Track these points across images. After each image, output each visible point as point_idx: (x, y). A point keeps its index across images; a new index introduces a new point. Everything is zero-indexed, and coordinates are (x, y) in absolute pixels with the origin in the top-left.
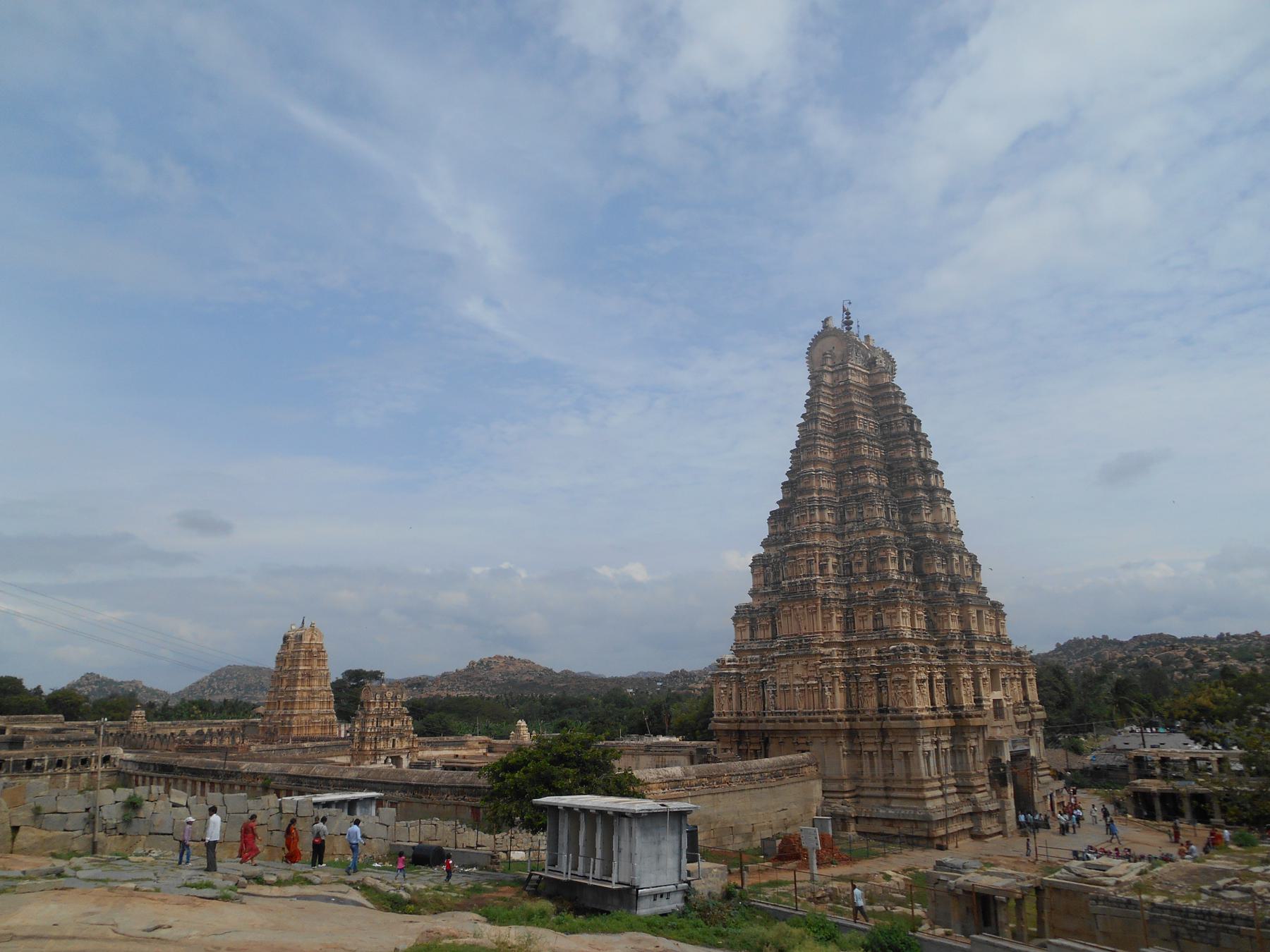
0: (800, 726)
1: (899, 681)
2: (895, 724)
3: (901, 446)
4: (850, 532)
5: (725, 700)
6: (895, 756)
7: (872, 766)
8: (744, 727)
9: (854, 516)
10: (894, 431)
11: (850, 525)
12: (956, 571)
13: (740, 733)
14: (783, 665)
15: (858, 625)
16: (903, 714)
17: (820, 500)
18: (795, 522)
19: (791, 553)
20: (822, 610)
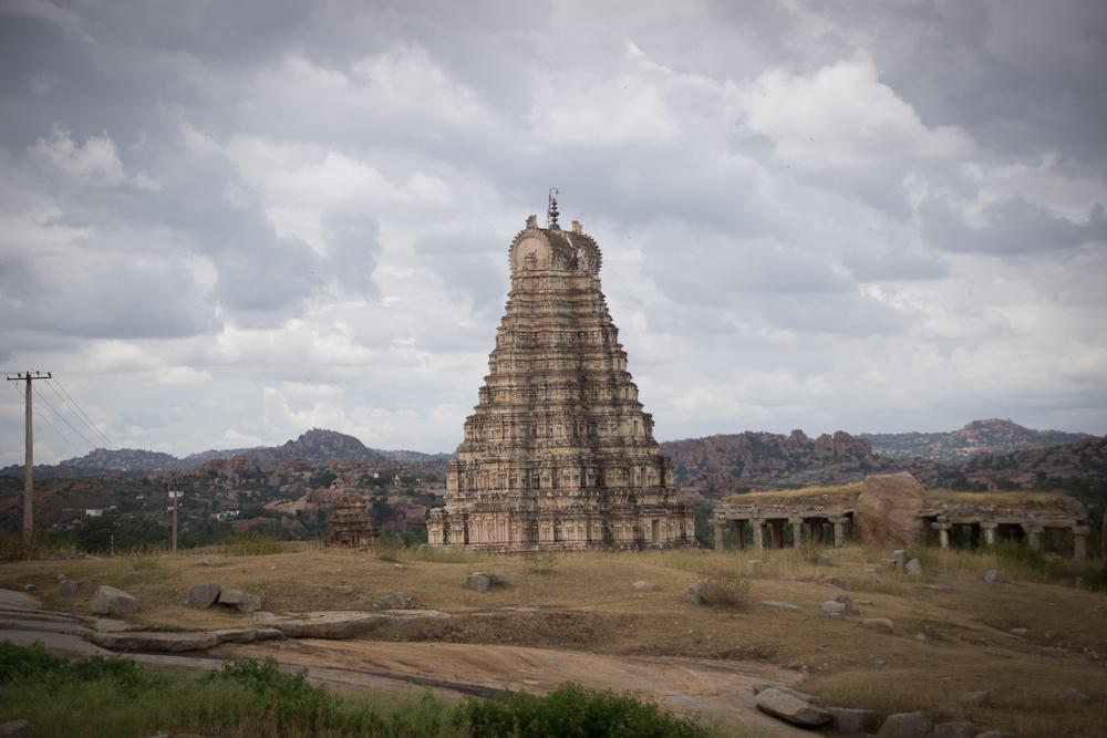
3: (596, 359)
10: (590, 341)
11: (540, 440)
12: (636, 483)
15: (542, 536)
17: (513, 416)
18: (490, 435)
20: (510, 522)
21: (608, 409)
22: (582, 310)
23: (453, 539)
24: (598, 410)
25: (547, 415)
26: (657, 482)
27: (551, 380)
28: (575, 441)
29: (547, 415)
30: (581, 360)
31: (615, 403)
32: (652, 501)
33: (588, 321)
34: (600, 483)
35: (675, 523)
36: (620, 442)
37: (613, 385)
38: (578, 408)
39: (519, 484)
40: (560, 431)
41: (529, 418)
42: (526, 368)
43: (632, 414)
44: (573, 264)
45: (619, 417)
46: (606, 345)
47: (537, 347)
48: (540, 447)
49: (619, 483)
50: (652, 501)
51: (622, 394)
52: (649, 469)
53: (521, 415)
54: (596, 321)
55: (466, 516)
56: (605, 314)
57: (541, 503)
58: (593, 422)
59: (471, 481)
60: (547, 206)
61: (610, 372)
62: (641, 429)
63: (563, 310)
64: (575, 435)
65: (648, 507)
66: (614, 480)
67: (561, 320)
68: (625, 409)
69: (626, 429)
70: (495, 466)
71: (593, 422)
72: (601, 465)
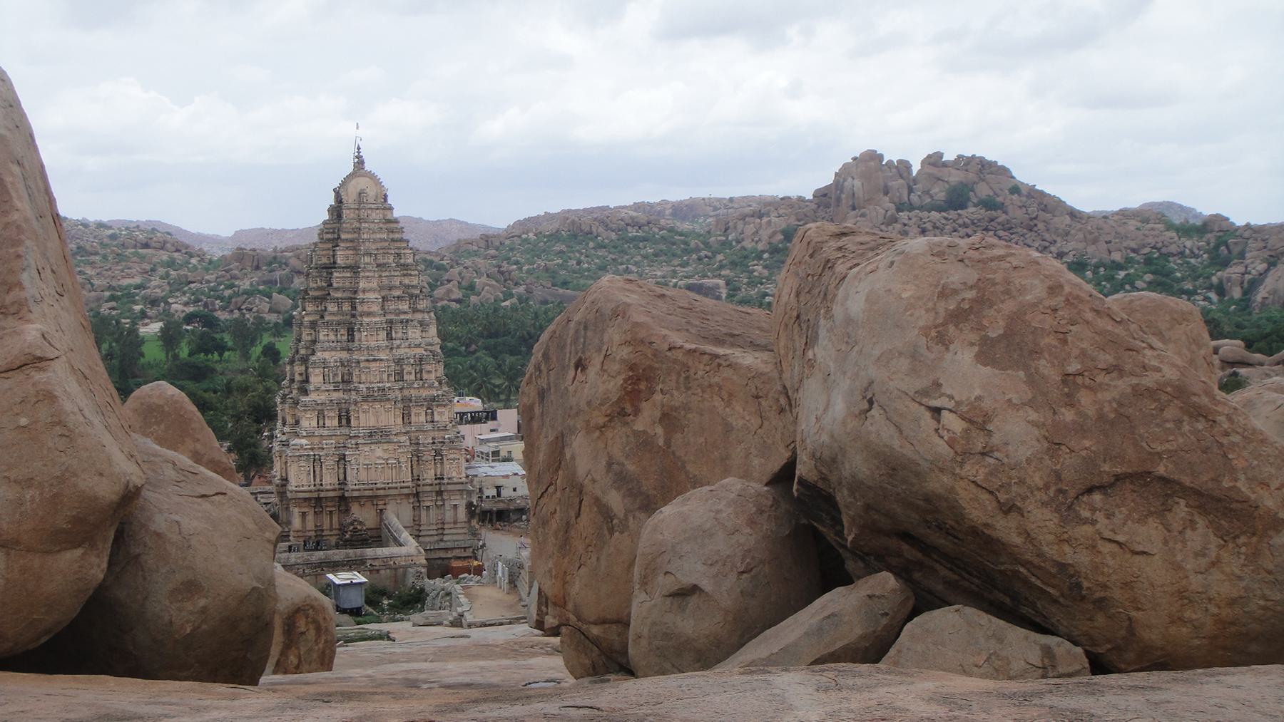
0: (382, 493)
1: (454, 459)
2: (450, 487)
4: (398, 347)
5: (304, 477)
6: (447, 506)
7: (428, 516)
8: (322, 494)
9: (400, 335)
11: (398, 342)
14: (367, 448)
15: (413, 419)
16: (455, 480)
19: (367, 364)
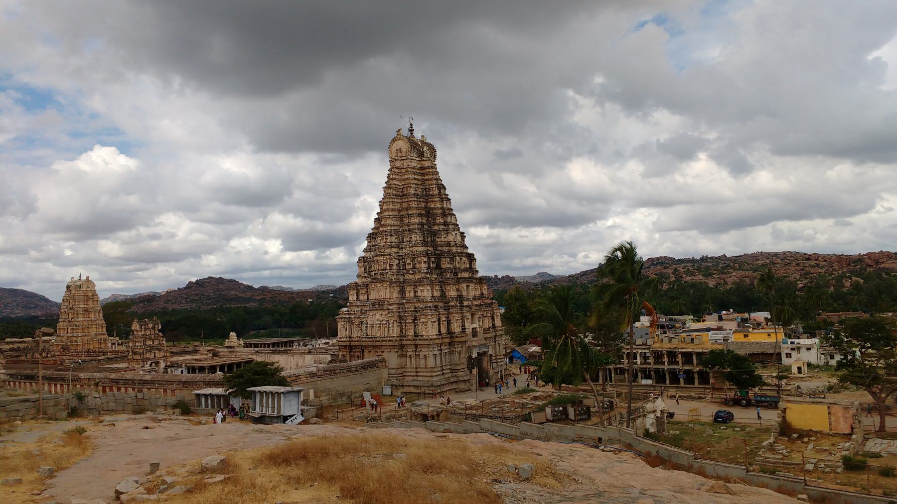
8: (352, 344)
13: (351, 347)
15: (407, 295)
21: (442, 227)
22: (426, 177)
23: (361, 297)
24: (436, 228)
25: (409, 230)
26: (468, 266)
27: (410, 212)
28: (424, 243)
29: (409, 230)
30: (427, 203)
31: (445, 224)
32: (466, 275)
33: (429, 182)
34: (438, 266)
35: (478, 287)
36: (448, 244)
37: (444, 215)
38: (426, 227)
39: (395, 267)
40: (417, 238)
41: (401, 233)
42: (398, 206)
43: (454, 230)
44: (421, 154)
45: (447, 232)
46: (440, 194)
47: (403, 195)
48: (406, 247)
49: (449, 266)
50: (466, 275)
51: (449, 220)
52: (464, 259)
53: (395, 230)
54: (435, 182)
55: (367, 285)
56: (438, 179)
57: (406, 277)
58: (435, 234)
59: (370, 267)
60: (408, 126)
61: (442, 208)
62: (459, 238)
63: (416, 177)
64: (424, 241)
65: (464, 278)
66: (446, 264)
67: (416, 182)
68: (451, 227)
69: (451, 238)
70: (382, 257)
71: (435, 234)
72: (438, 257)
